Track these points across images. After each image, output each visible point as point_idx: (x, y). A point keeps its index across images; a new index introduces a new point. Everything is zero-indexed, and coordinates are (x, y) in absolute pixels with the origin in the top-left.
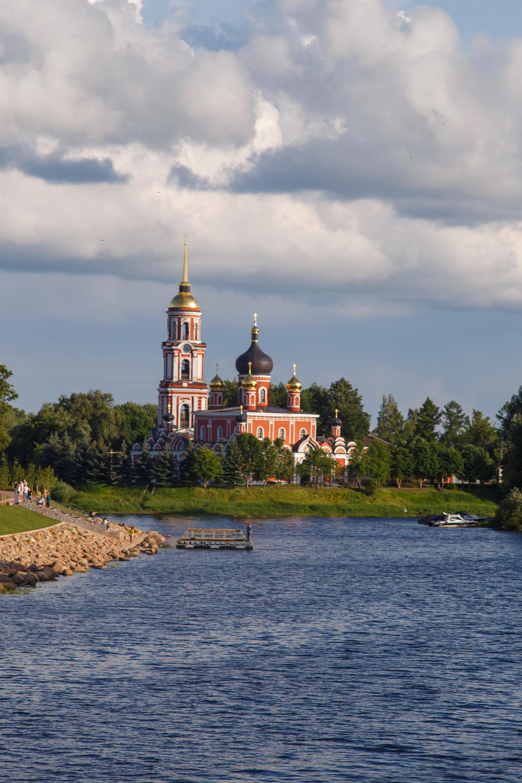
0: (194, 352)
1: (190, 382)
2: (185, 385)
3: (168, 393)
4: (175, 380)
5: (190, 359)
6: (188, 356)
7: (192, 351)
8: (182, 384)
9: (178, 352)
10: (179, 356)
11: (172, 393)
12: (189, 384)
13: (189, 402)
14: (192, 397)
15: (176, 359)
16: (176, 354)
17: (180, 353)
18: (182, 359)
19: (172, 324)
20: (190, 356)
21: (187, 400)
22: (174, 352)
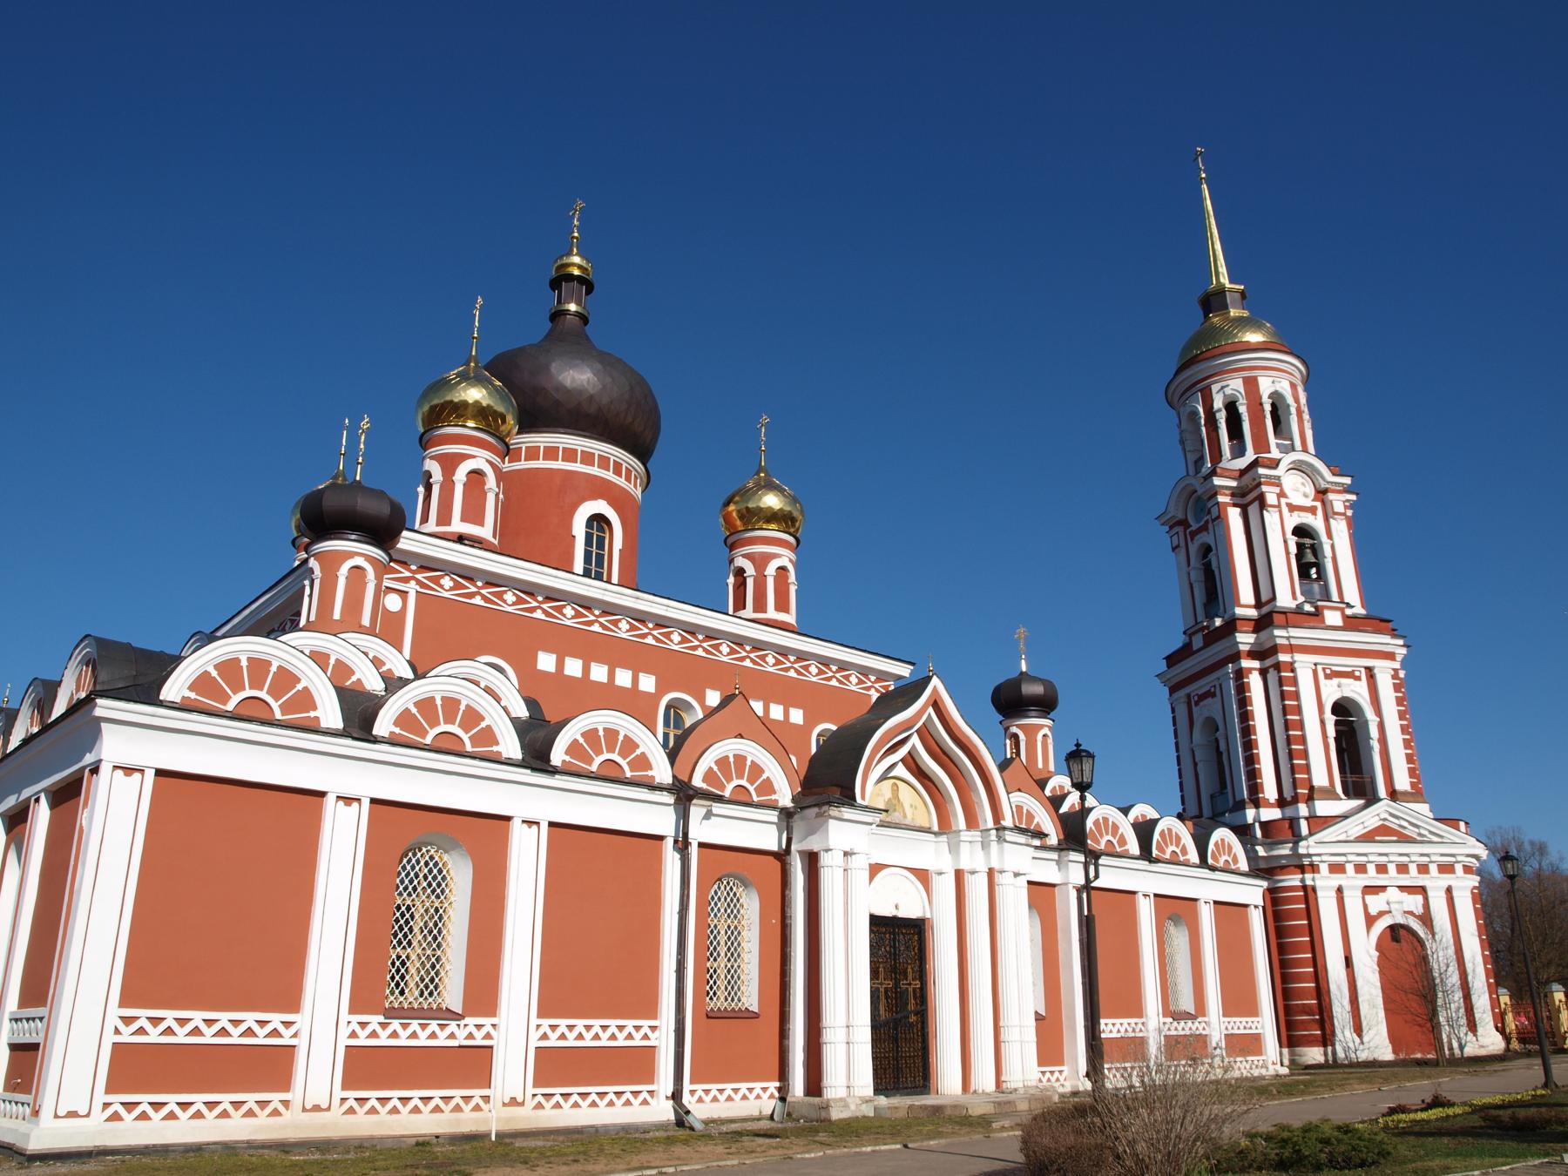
0: (1331, 496)
1: (1348, 612)
2: (1333, 618)
3: (1274, 650)
4: (1285, 600)
5: (1317, 522)
6: (1313, 510)
7: (1321, 493)
8: (1318, 614)
9: (1277, 490)
10: (1279, 506)
11: (1291, 649)
12: (1346, 618)
13: (1357, 691)
14: (1369, 670)
15: (1271, 518)
16: (1271, 498)
17: (1283, 501)
18: (1292, 520)
19: (1218, 403)
20: (1320, 512)
21: (1350, 681)
22: (1264, 488)
